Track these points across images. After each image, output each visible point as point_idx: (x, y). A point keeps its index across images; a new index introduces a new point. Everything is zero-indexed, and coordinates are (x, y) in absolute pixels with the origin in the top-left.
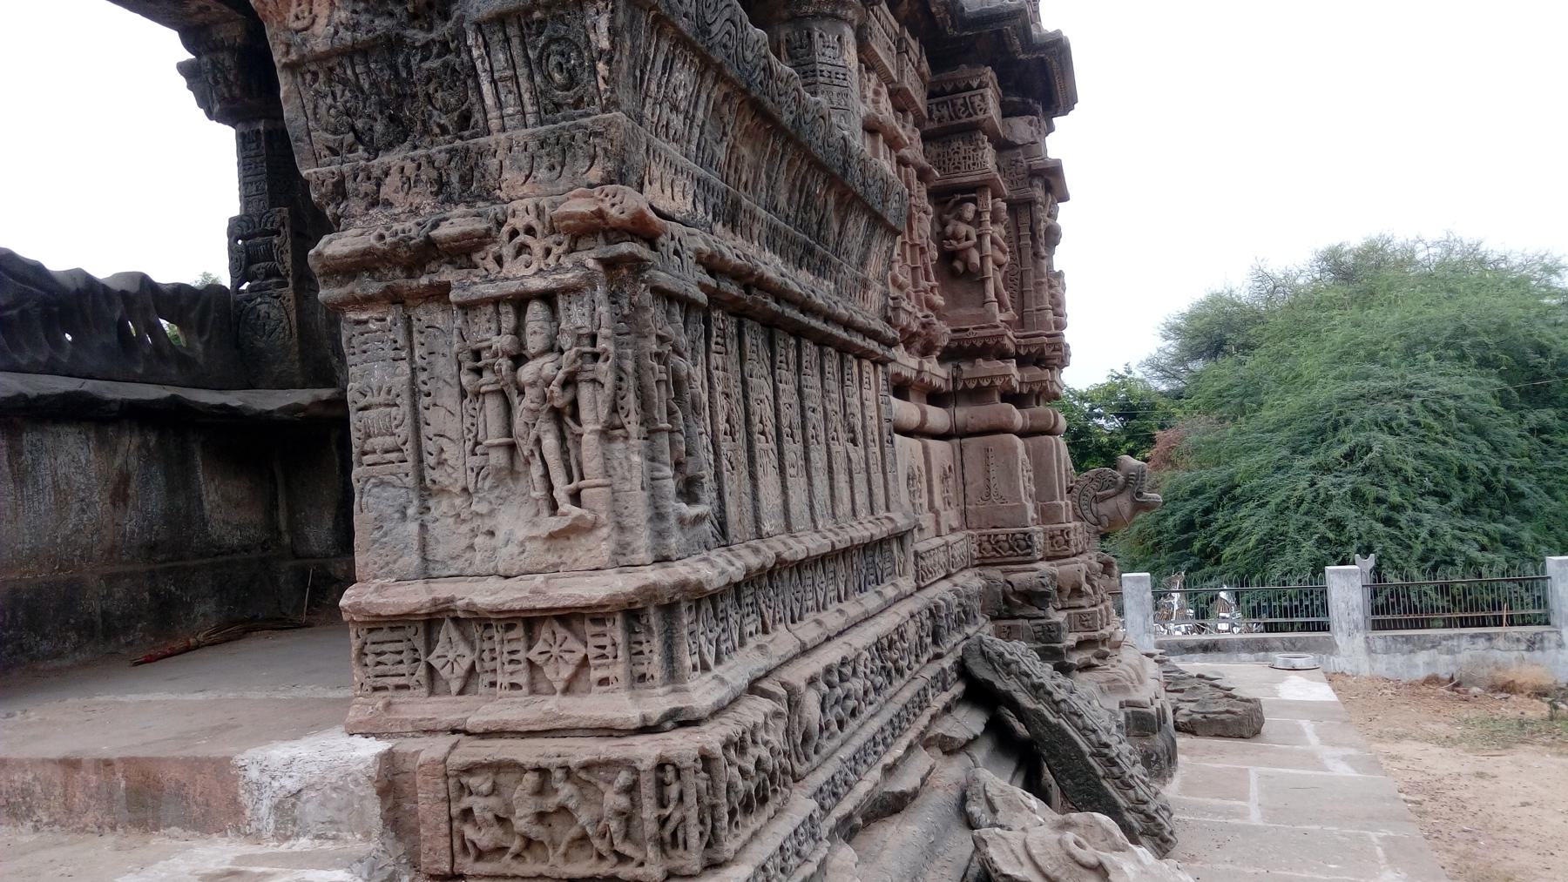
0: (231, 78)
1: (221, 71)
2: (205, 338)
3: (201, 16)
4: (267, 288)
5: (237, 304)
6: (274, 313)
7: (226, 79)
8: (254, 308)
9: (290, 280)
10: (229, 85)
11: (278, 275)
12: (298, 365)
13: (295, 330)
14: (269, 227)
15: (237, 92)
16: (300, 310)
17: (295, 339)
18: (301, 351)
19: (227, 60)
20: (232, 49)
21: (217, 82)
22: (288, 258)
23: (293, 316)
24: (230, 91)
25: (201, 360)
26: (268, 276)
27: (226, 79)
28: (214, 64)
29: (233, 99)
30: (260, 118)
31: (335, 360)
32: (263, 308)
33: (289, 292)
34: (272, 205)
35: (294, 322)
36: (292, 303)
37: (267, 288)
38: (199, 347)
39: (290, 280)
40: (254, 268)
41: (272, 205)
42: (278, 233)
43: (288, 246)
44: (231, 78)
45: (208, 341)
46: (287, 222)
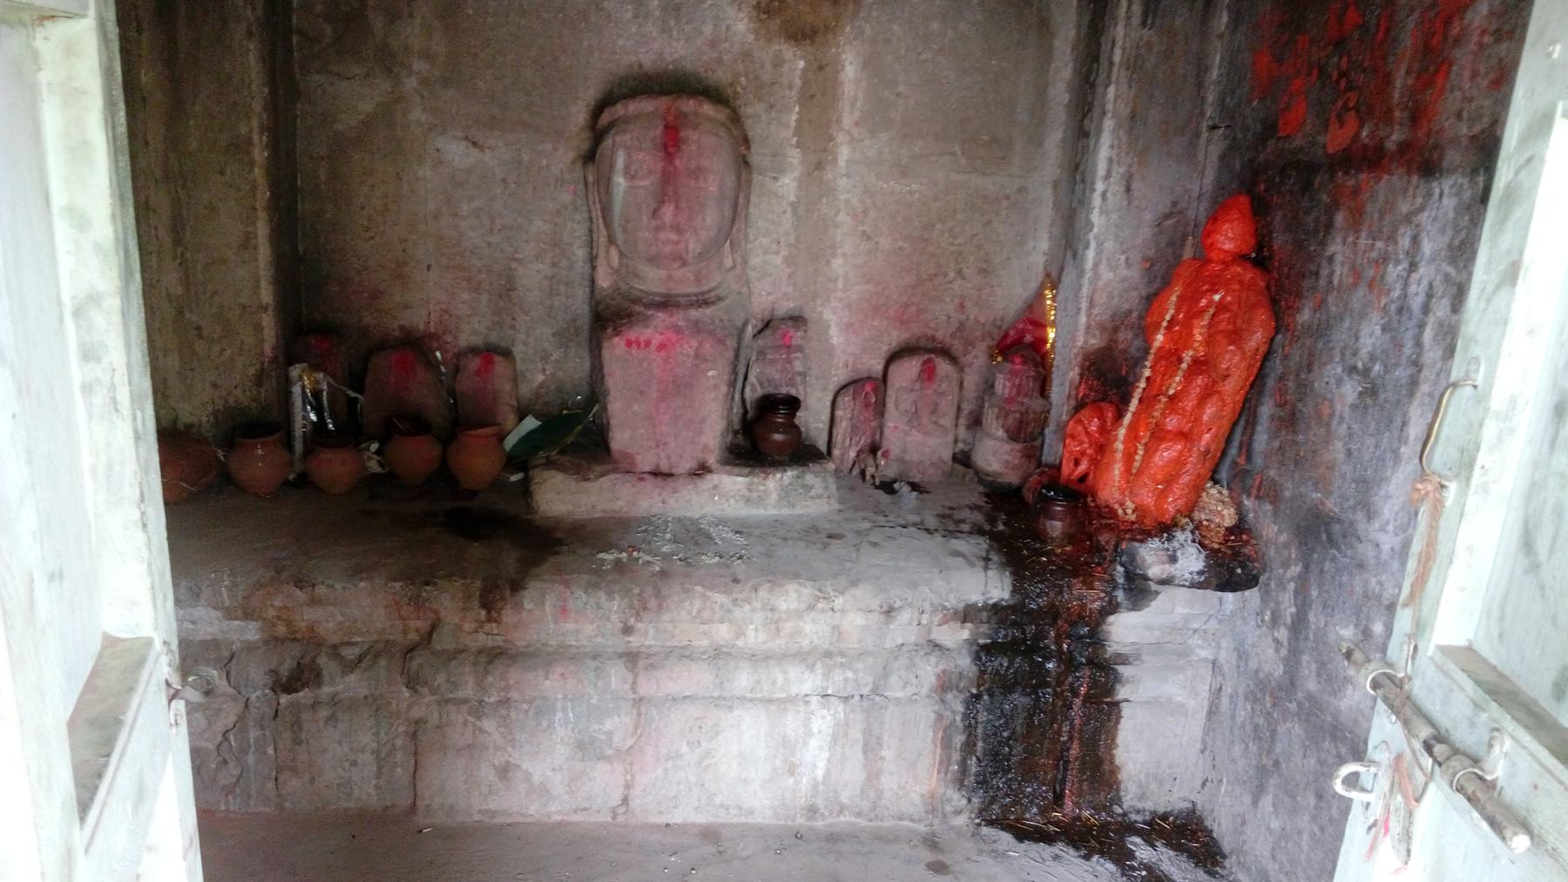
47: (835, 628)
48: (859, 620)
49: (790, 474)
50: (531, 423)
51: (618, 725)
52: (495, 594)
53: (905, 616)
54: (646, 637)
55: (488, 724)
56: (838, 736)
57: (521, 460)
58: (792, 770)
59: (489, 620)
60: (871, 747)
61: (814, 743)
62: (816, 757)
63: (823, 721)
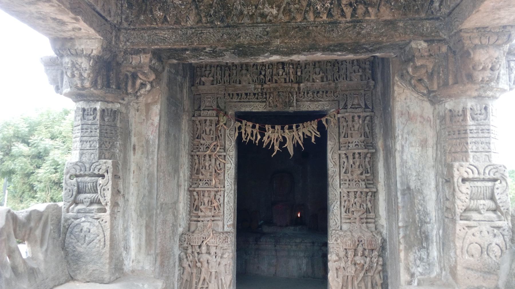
0: (85, 75)
1: (77, 69)
2: (45, 247)
3: (72, 33)
4: (90, 212)
5: (66, 220)
6: (93, 230)
7: (81, 75)
8: (79, 224)
9: (108, 208)
10: (82, 79)
11: (99, 203)
12: (107, 266)
13: (108, 243)
14: (96, 172)
15: (87, 84)
16: (112, 228)
17: (107, 248)
18: (111, 258)
19: (85, 64)
20: (89, 57)
21: (73, 76)
22: (108, 194)
23: (108, 233)
24: (82, 83)
25: (42, 267)
26: (92, 203)
27: (81, 75)
28: (73, 65)
29: (83, 88)
30: (98, 101)
31: (124, 254)
32: (86, 226)
33: (106, 216)
34: (100, 158)
35: (108, 237)
36: (108, 225)
37: (90, 212)
38: (41, 256)
39: (108, 208)
40: (82, 196)
41: (100, 158)
42: (103, 176)
43: (110, 186)
44: (85, 75)
45: (46, 250)
46: (110, 170)
47: (306, 246)
48: (309, 244)
49: (300, 227)
50: (262, 222)
51: (274, 261)
52: (257, 240)
53: (316, 244)
54: (278, 247)
55: (256, 260)
56: (307, 264)
57: (260, 226)
58: (300, 269)
59: (256, 244)
60: (313, 266)
61: (303, 265)
62: (304, 267)
63: (305, 261)
